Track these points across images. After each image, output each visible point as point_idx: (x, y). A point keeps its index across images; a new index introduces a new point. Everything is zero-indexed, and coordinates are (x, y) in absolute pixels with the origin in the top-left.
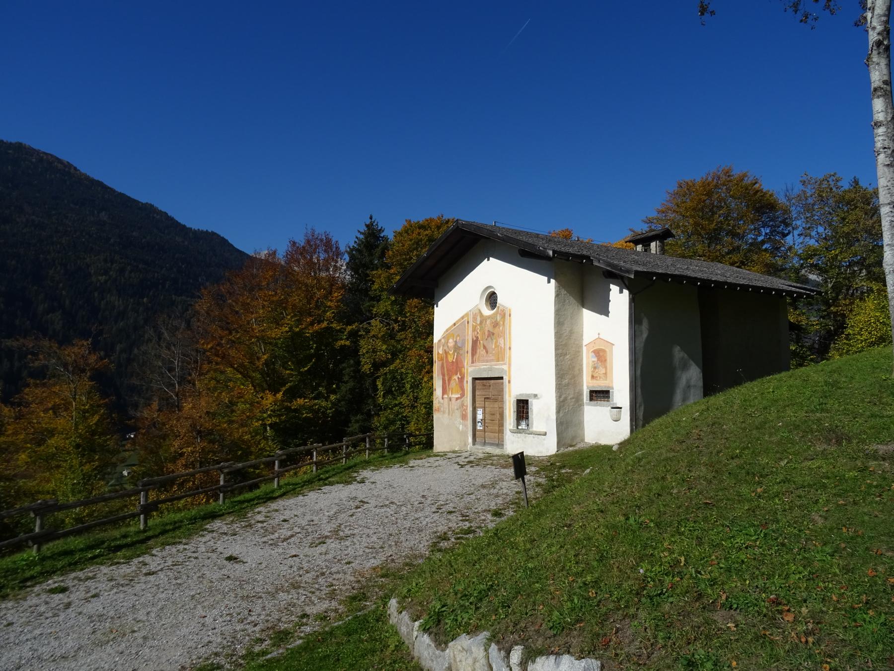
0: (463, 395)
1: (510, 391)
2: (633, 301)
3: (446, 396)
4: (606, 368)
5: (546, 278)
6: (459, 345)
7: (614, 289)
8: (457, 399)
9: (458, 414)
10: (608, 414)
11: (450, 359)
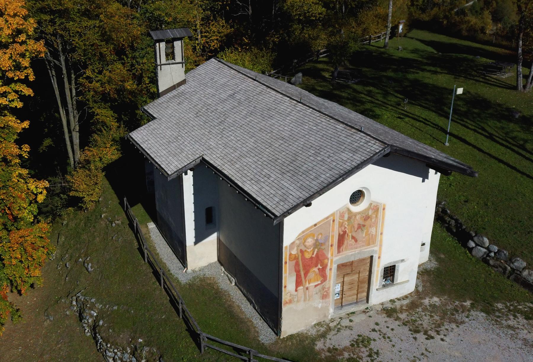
3: (301, 288)
8: (316, 286)
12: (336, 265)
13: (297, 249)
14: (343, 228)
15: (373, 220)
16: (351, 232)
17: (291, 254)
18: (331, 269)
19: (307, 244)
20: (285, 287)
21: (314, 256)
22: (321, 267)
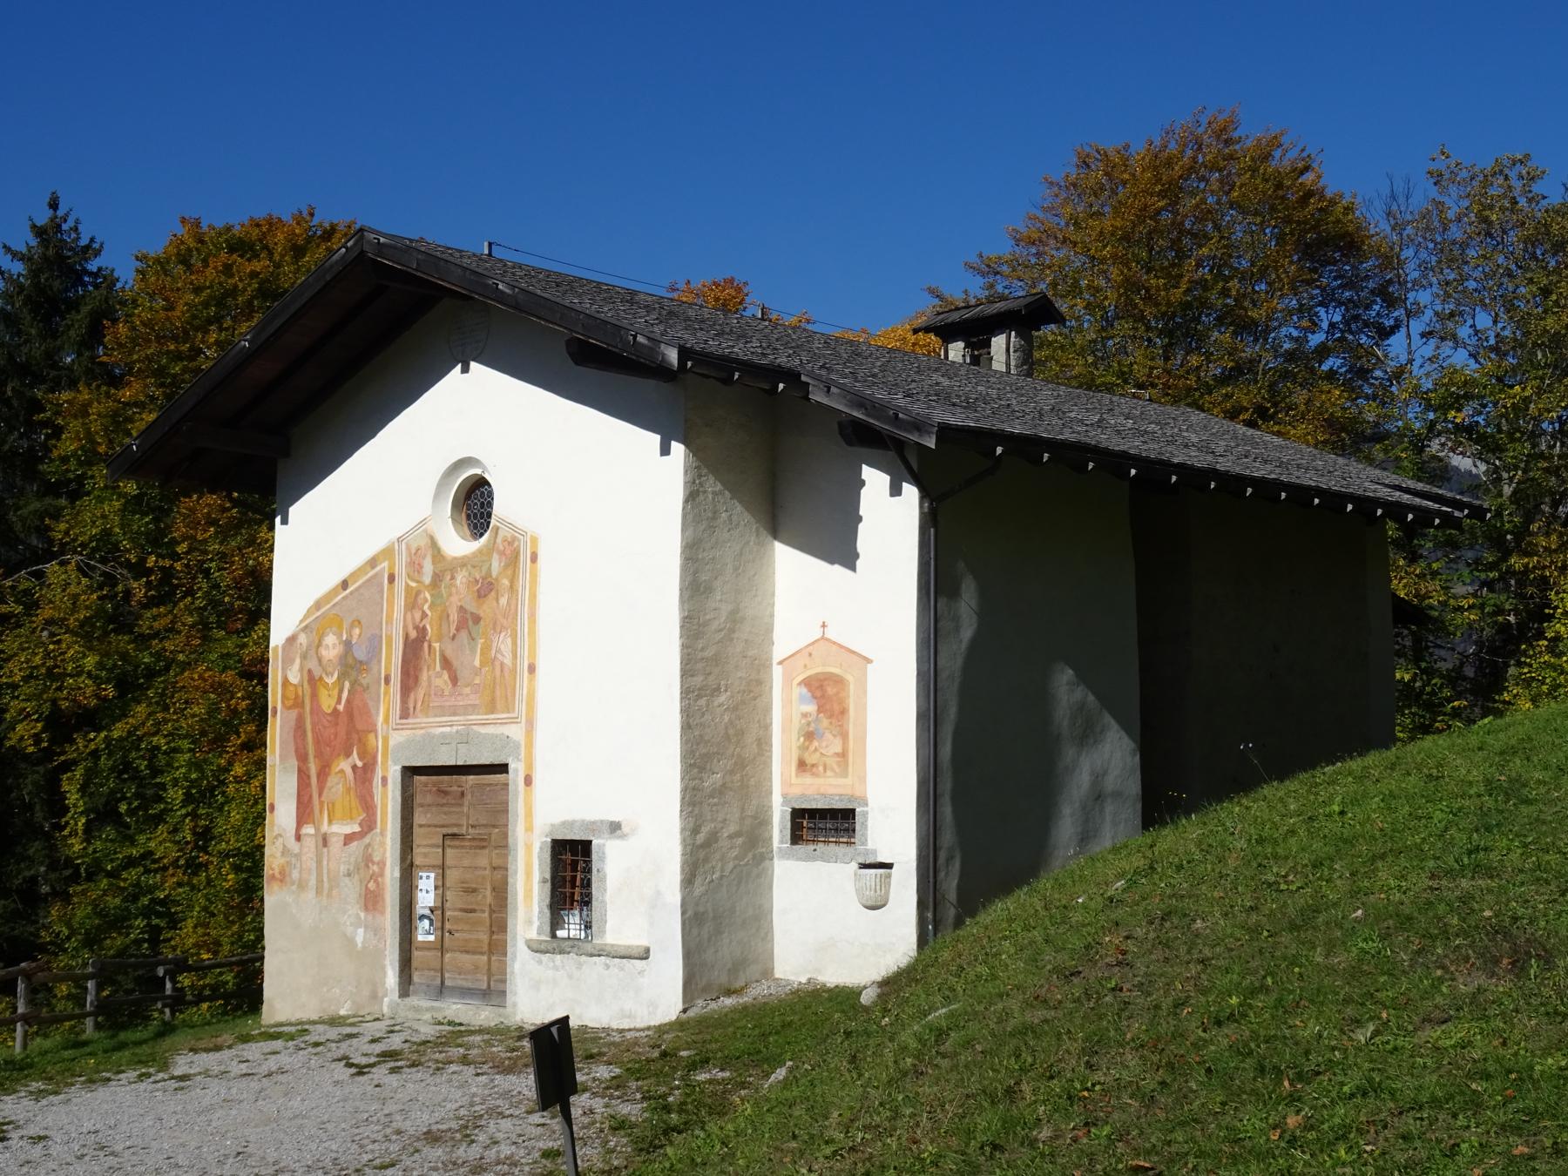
0: (369, 825)
1: (529, 814)
2: (931, 521)
3: (308, 830)
4: (844, 736)
5: (657, 438)
6: (360, 654)
7: (875, 480)
8: (349, 839)
9: (351, 890)
10: (850, 887)
11: (327, 703)
12: (398, 768)
13: (301, 669)
14: (418, 615)
15: (503, 601)
16: (440, 640)
17: (286, 682)
18: (384, 780)
19: (324, 652)
20: (272, 807)
21: (341, 708)
22: (360, 764)
